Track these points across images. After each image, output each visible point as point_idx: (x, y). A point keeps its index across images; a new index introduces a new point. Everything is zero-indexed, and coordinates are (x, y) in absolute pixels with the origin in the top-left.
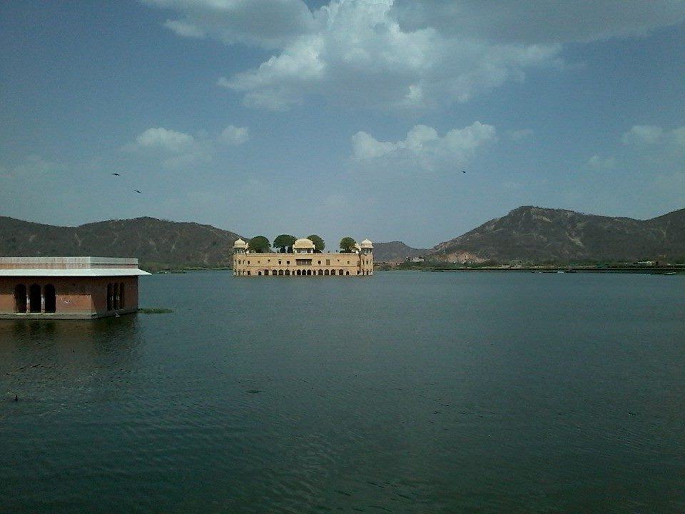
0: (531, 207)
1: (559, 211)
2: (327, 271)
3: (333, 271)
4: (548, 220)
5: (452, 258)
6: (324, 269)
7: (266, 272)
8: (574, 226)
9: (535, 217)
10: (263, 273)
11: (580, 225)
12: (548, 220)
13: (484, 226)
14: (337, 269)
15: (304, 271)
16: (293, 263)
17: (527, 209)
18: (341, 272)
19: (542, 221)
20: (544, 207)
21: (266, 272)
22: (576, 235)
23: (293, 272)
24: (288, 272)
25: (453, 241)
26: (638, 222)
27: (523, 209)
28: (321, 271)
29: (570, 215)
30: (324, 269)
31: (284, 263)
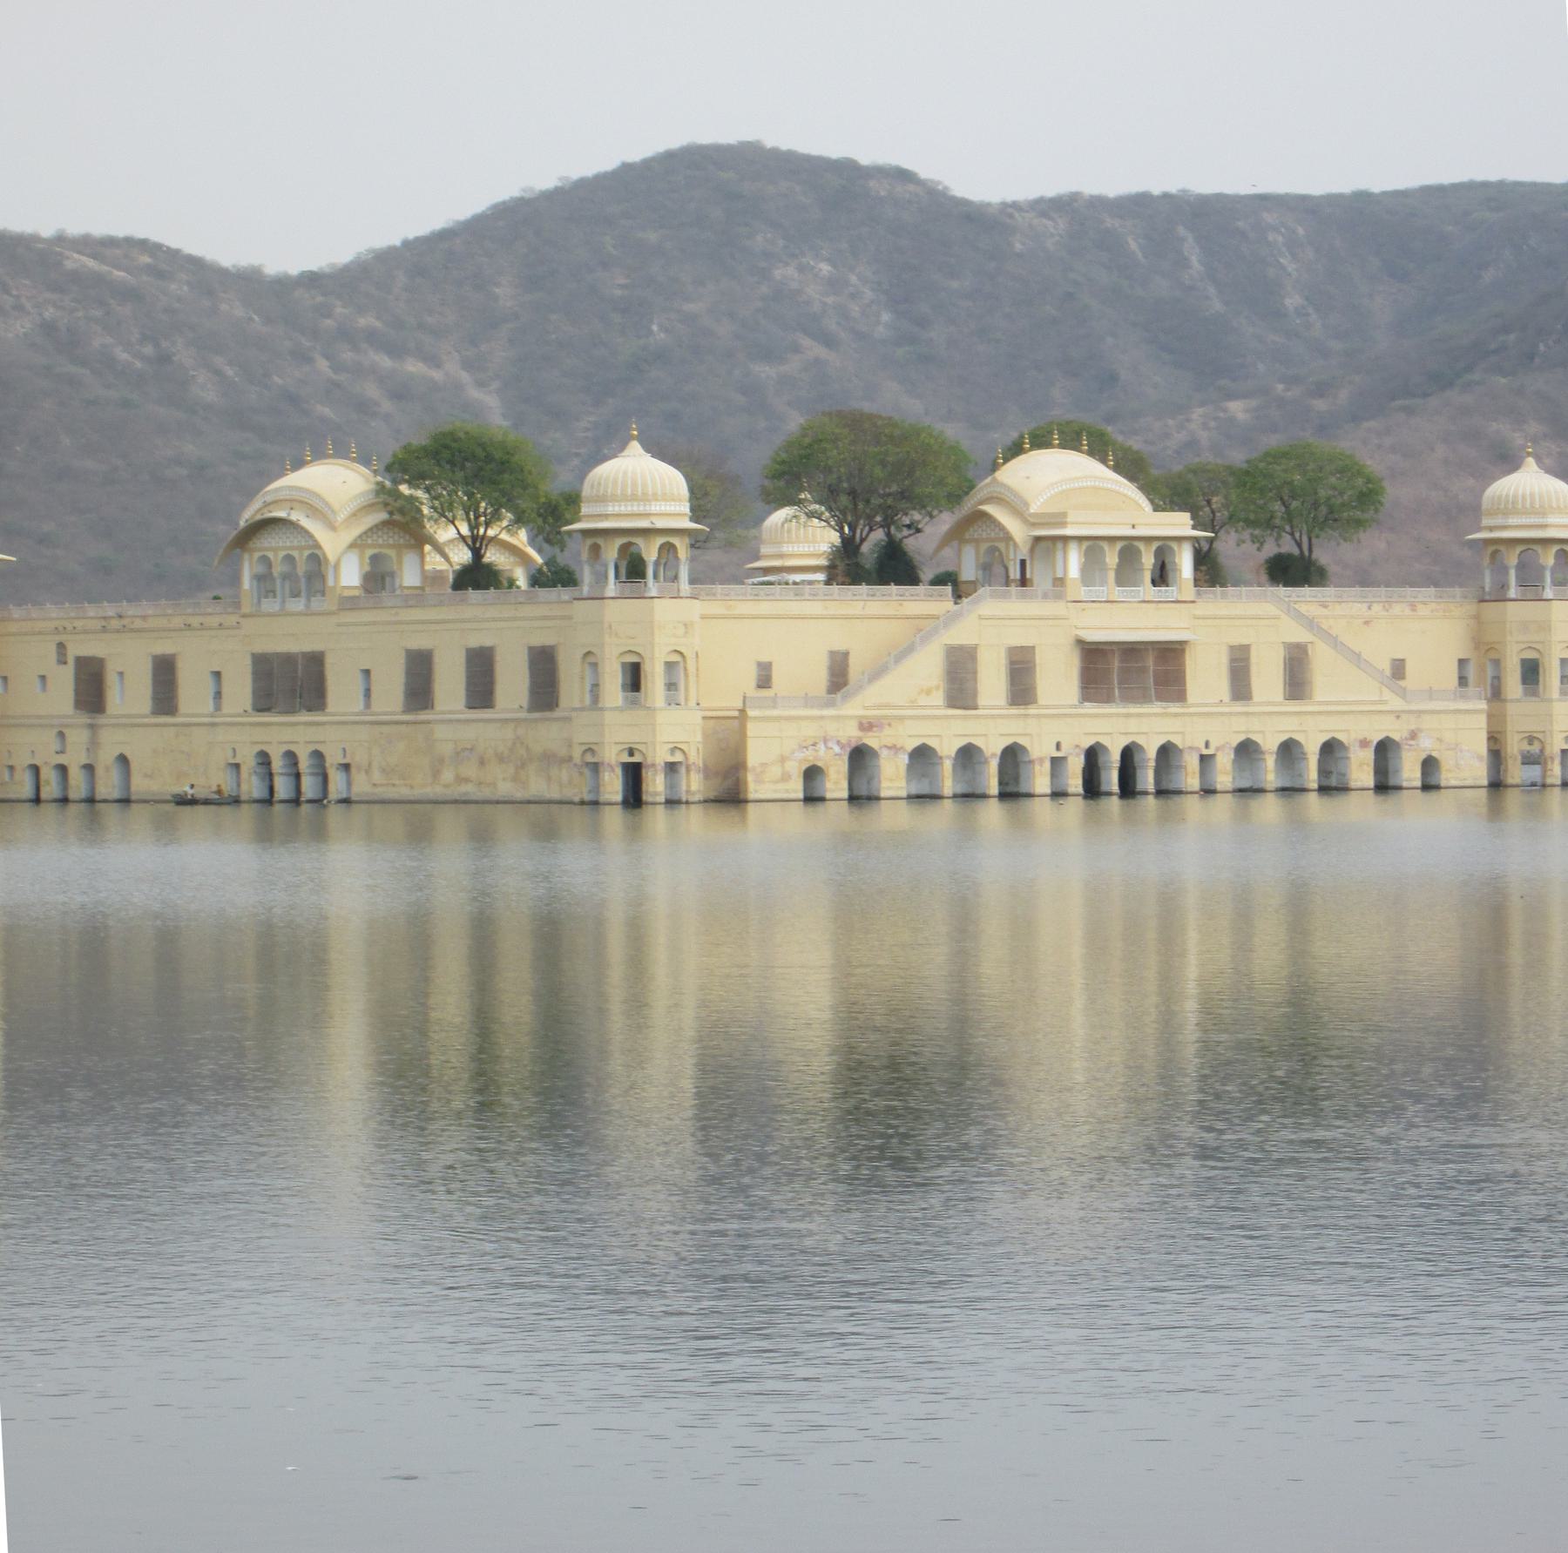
2: (1289, 751)
3: (1330, 749)
6: (1270, 743)
7: (860, 757)
10: (836, 784)
14: (1359, 733)
15: (1129, 755)
16: (1058, 677)
18: (1385, 750)
21: (860, 757)
23: (1057, 763)
24: (1012, 757)
26: (249, 284)
28: (1246, 751)
30: (1270, 743)
31: (992, 682)
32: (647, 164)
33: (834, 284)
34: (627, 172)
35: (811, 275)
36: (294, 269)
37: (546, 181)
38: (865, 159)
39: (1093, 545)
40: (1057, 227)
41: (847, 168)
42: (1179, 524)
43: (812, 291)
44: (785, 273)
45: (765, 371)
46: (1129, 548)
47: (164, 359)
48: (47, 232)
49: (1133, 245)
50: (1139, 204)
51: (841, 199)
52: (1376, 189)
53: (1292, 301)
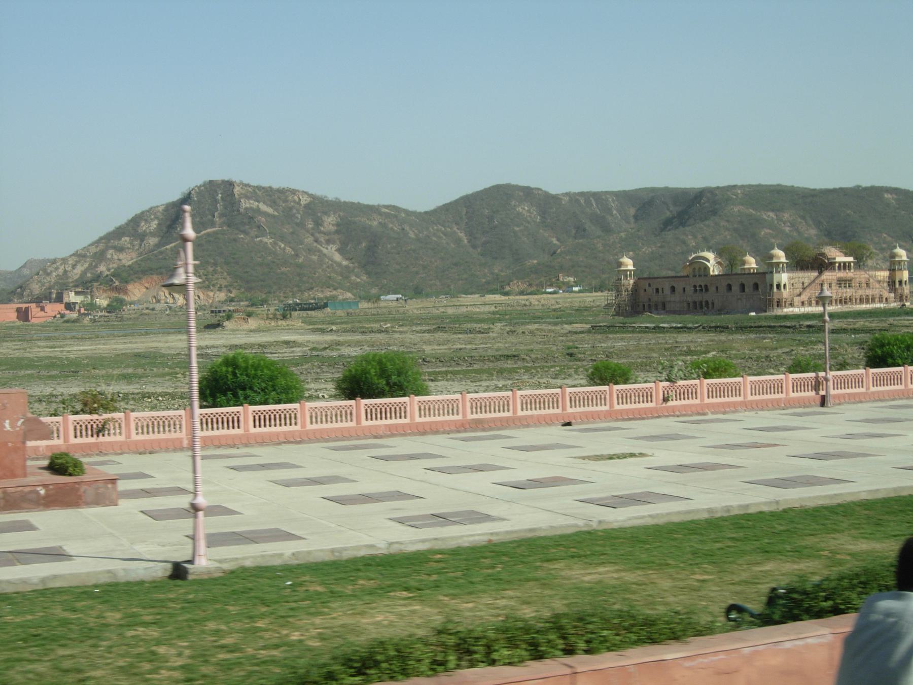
0: (230, 184)
1: (282, 191)
4: (270, 210)
5: (136, 291)
8: (318, 223)
9: (245, 204)
11: (330, 222)
12: (270, 210)
13: (136, 220)
17: (229, 185)
19: (258, 211)
20: (254, 183)
22: (328, 242)
25: (80, 256)
26: (414, 213)
27: (211, 186)
29: (305, 200)
32: (490, 188)
33: (529, 211)
34: (486, 190)
35: (524, 209)
36: (422, 210)
37: (470, 192)
38: (533, 186)
39: (840, 263)
40: (567, 199)
41: (528, 188)
42: (851, 259)
43: (524, 212)
44: (519, 209)
45: (517, 229)
46: (845, 263)
47: (403, 229)
48: (376, 204)
49: (582, 202)
50: (582, 194)
51: (528, 193)
52: (627, 189)
53: (615, 212)
